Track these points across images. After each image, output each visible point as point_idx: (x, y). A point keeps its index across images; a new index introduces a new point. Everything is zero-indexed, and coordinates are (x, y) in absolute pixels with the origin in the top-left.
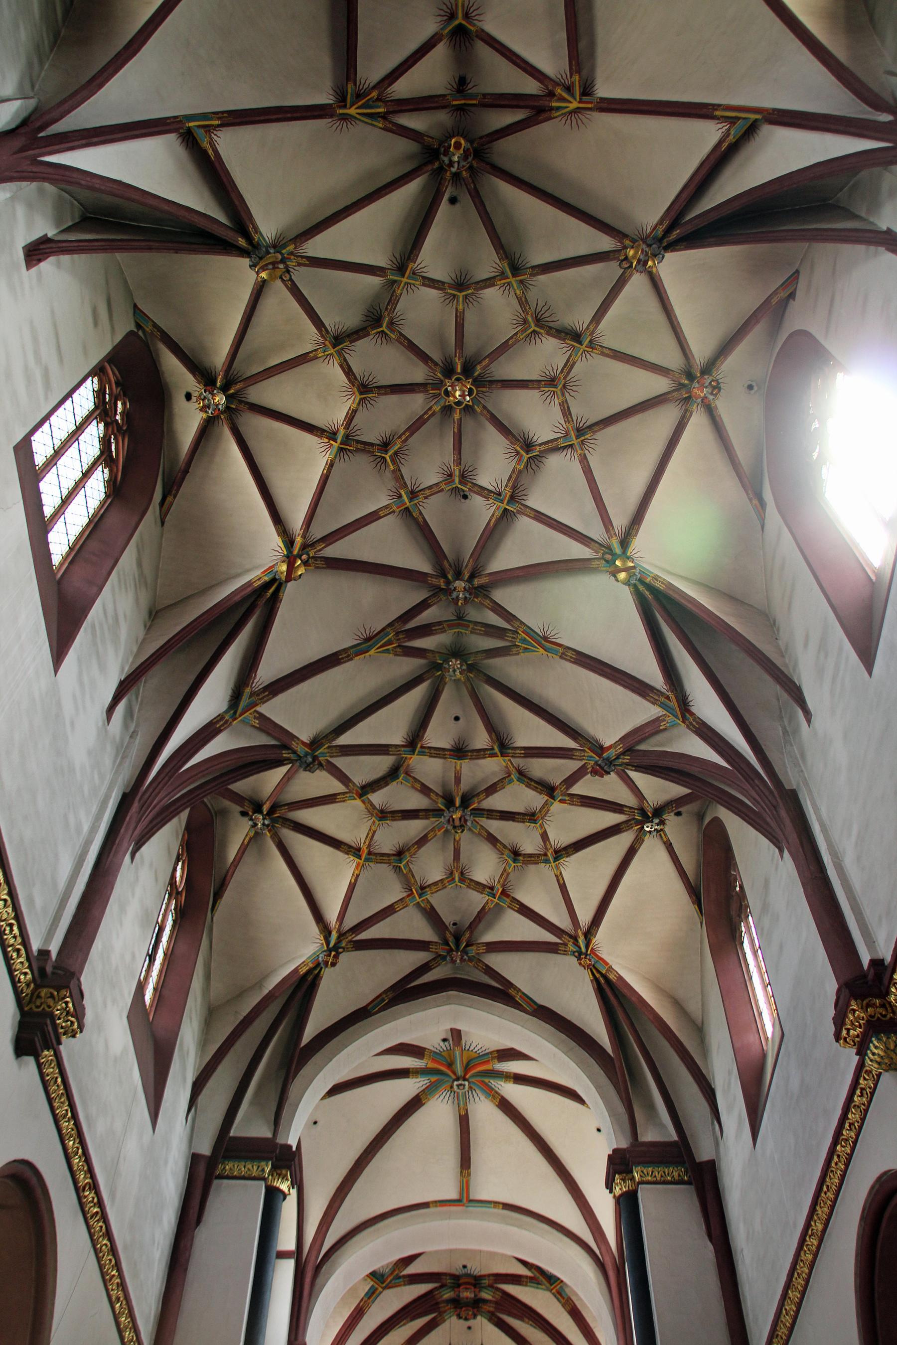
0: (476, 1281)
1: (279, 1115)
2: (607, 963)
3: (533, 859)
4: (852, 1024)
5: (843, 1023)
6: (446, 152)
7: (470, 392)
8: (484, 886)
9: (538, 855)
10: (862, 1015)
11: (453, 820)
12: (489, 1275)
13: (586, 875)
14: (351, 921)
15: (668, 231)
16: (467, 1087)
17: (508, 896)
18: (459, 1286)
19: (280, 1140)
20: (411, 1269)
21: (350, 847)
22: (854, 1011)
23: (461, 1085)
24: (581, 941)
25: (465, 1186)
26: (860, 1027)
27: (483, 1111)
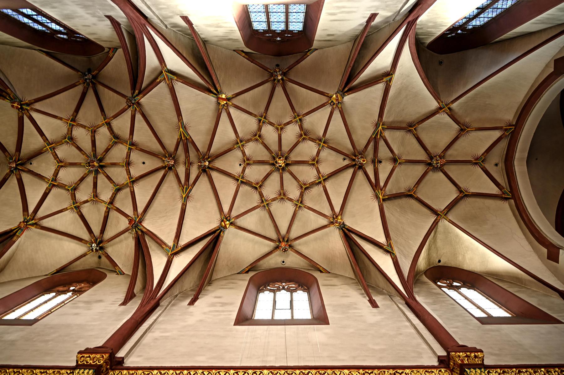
2: (21, 235)
3: (74, 197)
6: (362, 157)
7: (281, 166)
8: (56, 176)
9: (75, 199)
11: (93, 162)
13: (67, 221)
14: (35, 115)
15: (347, 229)
17: (52, 187)
21: (76, 117)
24: (33, 222)
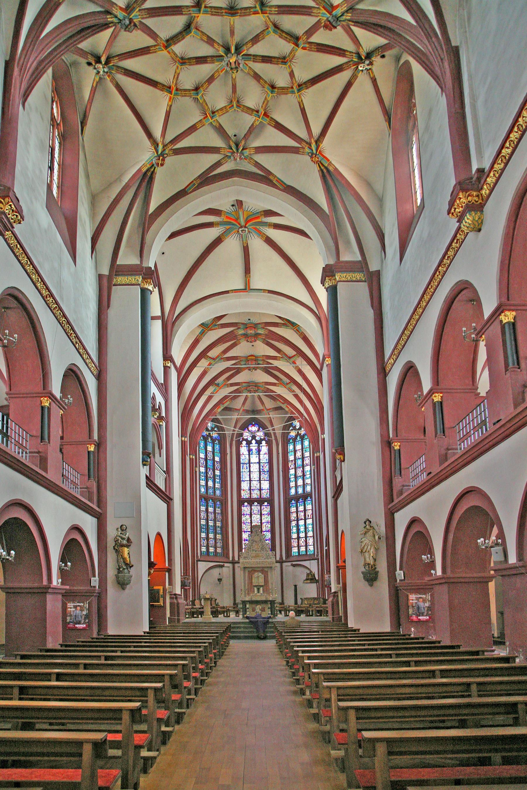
0: (255, 326)
1: (142, 251)
4: (458, 205)
5: (453, 205)
10: (464, 201)
12: (262, 323)
16: (247, 231)
18: (247, 328)
19: (144, 265)
20: (222, 321)
21: (164, 85)
22: (460, 198)
23: (243, 230)
25: (247, 283)
26: (462, 207)
27: (257, 245)
